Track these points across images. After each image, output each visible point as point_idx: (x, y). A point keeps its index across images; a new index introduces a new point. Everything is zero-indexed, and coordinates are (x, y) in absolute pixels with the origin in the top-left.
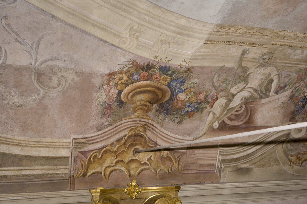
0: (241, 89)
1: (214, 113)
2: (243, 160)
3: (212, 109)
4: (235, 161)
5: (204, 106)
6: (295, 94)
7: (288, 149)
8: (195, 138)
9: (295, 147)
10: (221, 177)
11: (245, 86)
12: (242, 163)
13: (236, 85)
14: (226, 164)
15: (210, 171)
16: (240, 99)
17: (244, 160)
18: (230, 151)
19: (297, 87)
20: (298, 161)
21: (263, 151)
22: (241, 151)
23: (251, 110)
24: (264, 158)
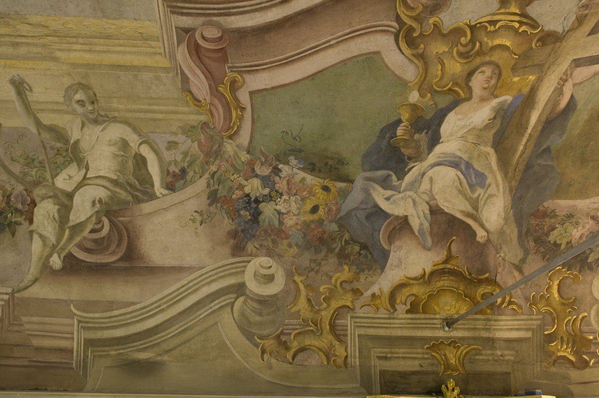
0: (79, 181)
1: (41, 236)
2: (138, 343)
3: (32, 226)
4: (118, 344)
5: (13, 220)
6: (218, 190)
7: (249, 322)
8: (16, 290)
9: (268, 317)
10: (88, 379)
11: (86, 174)
12: (135, 348)
13: (62, 170)
14: (98, 349)
15: (61, 363)
16: (88, 205)
17: (140, 342)
18: (102, 320)
19: (215, 172)
20: (283, 351)
21: (185, 324)
22: (129, 321)
23: (127, 230)
24: (189, 341)
